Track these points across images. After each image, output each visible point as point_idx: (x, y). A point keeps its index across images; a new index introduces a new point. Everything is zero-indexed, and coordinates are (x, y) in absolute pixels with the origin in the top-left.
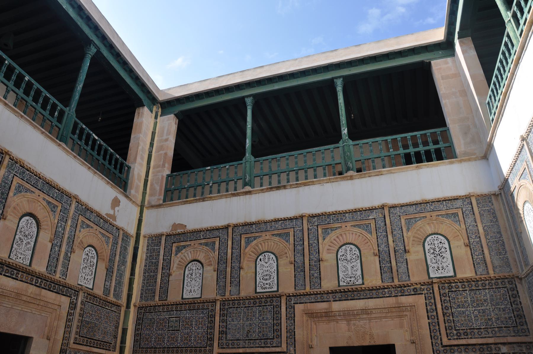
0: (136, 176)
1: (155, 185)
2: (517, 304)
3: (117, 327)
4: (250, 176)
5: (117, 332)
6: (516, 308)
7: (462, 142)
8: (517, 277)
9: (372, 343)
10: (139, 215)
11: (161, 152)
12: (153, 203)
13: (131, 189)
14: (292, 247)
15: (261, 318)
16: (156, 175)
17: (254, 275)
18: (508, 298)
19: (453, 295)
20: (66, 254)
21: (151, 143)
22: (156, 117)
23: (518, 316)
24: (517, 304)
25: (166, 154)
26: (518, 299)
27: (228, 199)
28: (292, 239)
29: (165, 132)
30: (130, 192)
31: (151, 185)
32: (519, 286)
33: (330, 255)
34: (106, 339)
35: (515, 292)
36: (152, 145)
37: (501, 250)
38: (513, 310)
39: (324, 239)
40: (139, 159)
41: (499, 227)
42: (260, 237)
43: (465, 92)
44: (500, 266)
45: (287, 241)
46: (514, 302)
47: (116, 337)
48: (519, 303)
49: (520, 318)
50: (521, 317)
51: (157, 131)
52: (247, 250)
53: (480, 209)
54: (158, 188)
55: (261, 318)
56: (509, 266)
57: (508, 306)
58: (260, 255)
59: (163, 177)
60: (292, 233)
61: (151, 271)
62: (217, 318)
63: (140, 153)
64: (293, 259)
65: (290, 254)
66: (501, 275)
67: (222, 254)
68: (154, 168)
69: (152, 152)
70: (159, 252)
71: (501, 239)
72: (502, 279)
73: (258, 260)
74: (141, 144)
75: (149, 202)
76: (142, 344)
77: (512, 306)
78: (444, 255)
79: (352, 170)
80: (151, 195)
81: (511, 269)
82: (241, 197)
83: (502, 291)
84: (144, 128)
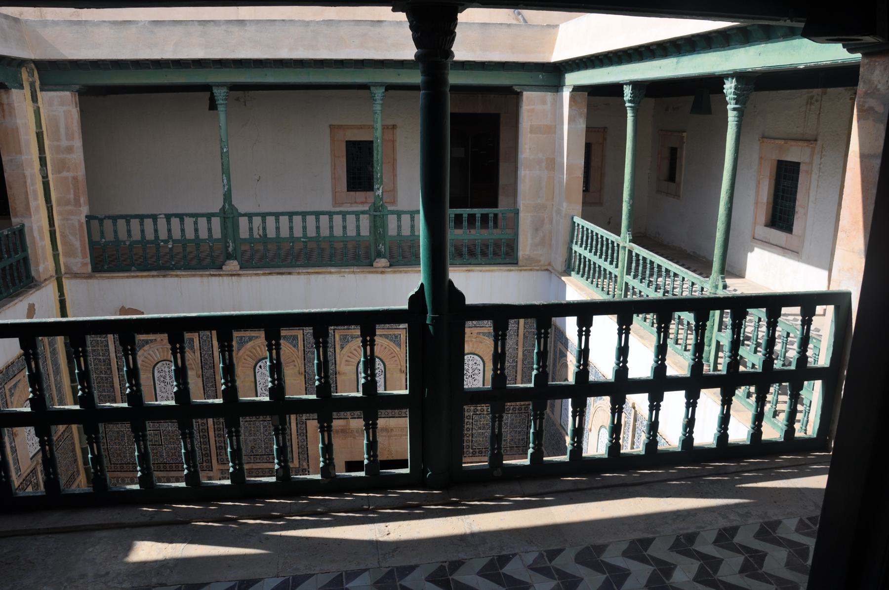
0: (36, 234)
1: (71, 237)
3: (74, 450)
4: (234, 242)
5: (75, 455)
7: (530, 241)
9: (390, 458)
10: (57, 294)
11: (65, 174)
12: (76, 269)
13: (37, 265)
14: (301, 353)
15: (266, 433)
16: (67, 220)
17: (253, 385)
19: (476, 418)
20: (11, 447)
21: (40, 158)
22: (34, 99)
25: (75, 179)
27: (205, 279)
28: (300, 343)
29: (62, 130)
30: (37, 271)
31: (63, 236)
33: (349, 368)
34: (70, 473)
36: (43, 161)
39: (342, 348)
40: (33, 204)
42: (257, 337)
43: (552, 164)
45: (294, 346)
47: (76, 461)
51: (44, 129)
52: (241, 353)
54: (77, 244)
55: (266, 433)
58: (259, 361)
59: (81, 224)
60: (300, 337)
61: (101, 372)
62: (212, 434)
63: (30, 190)
64: (303, 370)
65: (299, 362)
67: (206, 356)
68: (59, 205)
69: (47, 176)
70: (107, 346)
73: (258, 367)
74: (28, 172)
75: (66, 266)
76: (114, 460)
78: (476, 377)
79: (384, 257)
80: (68, 254)
82: (225, 278)
83: (523, 416)
84: (23, 138)
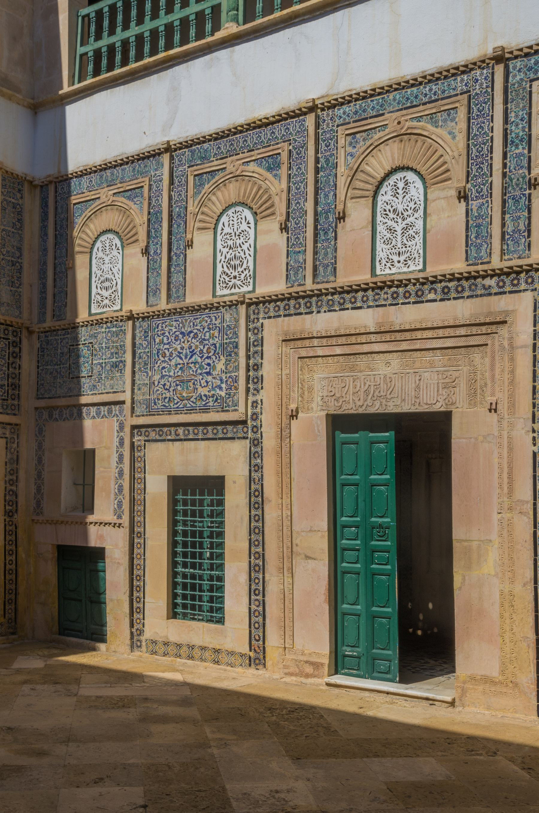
2: (15, 368)
6: (13, 373)
8: (28, 328)
18: (7, 356)
23: (11, 386)
24: (15, 368)
26: (18, 360)
32: (25, 342)
35: (17, 350)
37: (16, 278)
38: (8, 375)
41: (21, 240)
44: (8, 305)
46: (12, 364)
48: (17, 367)
49: (13, 389)
50: (16, 387)
53: (3, 197)
56: (19, 307)
57: (4, 368)
66: (7, 318)
71: (19, 260)
72: (7, 325)
77: (8, 370)
81: (20, 313)
